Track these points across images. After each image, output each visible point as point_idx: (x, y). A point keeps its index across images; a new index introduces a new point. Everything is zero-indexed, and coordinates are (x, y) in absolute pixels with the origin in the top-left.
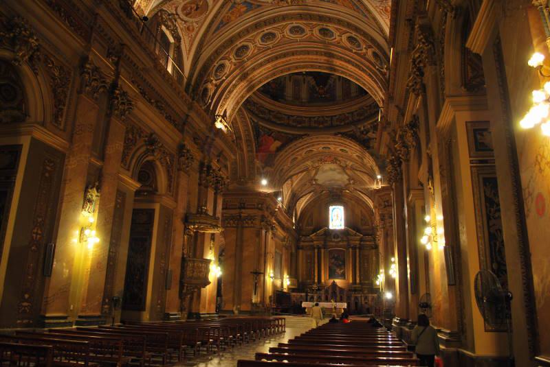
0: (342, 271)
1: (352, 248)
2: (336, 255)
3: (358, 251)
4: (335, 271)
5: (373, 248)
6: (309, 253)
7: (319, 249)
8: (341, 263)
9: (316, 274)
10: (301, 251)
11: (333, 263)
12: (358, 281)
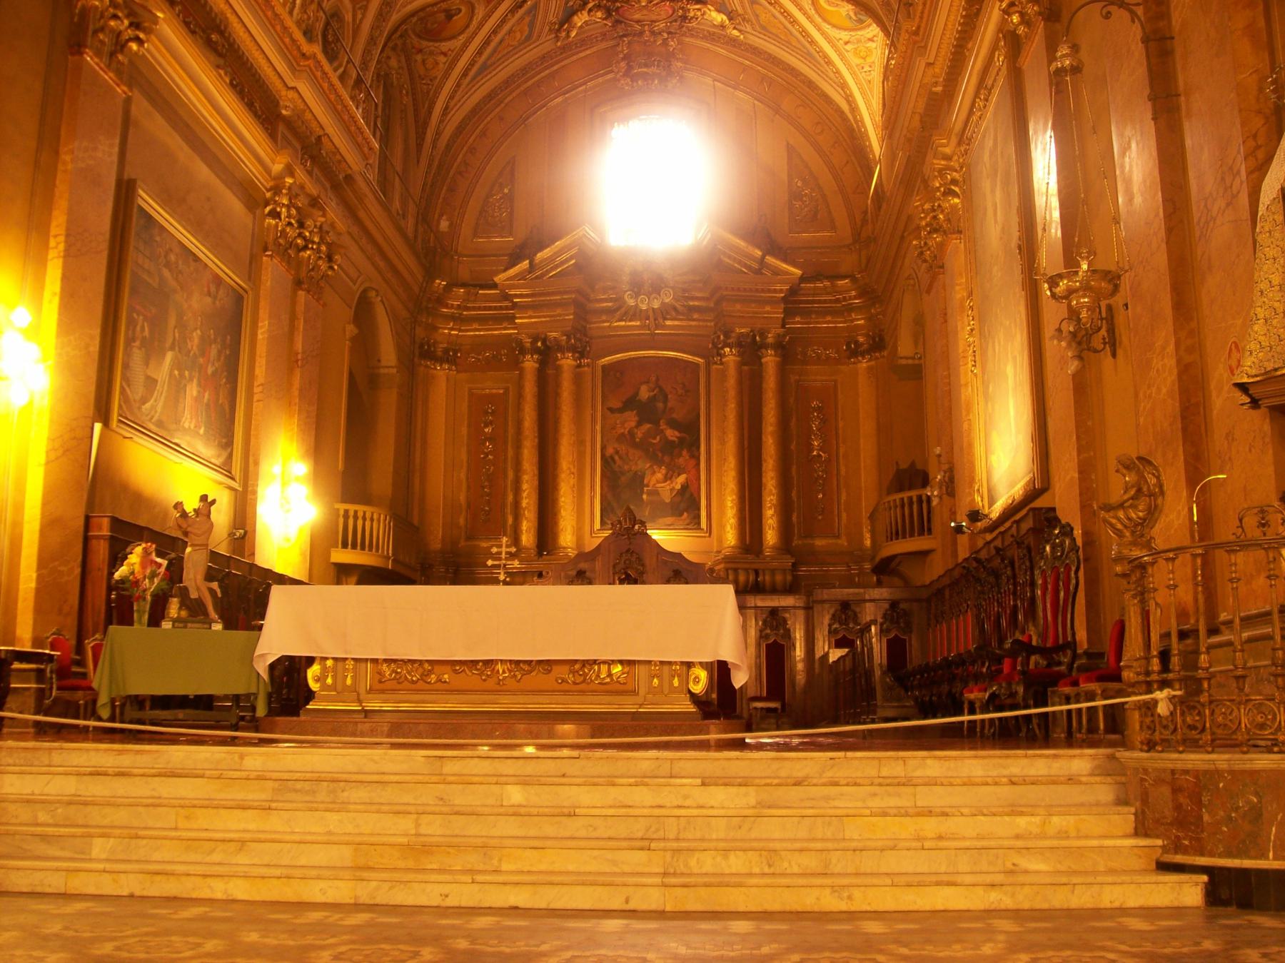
0: (681, 479)
1: (739, 345)
2: (644, 393)
3: (770, 360)
4: (638, 481)
5: (855, 352)
6: (491, 385)
7: (547, 353)
8: (672, 434)
9: (528, 500)
10: (441, 372)
11: (629, 438)
12: (771, 536)
